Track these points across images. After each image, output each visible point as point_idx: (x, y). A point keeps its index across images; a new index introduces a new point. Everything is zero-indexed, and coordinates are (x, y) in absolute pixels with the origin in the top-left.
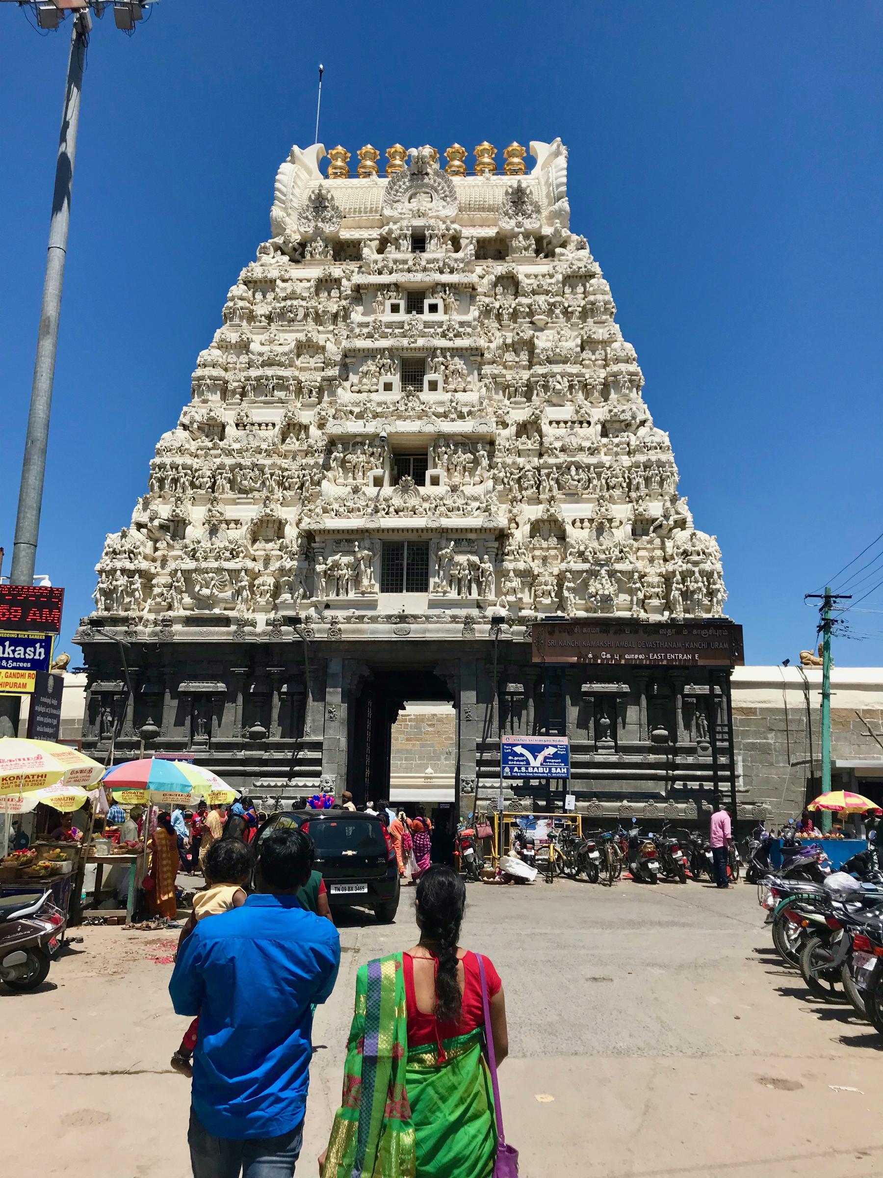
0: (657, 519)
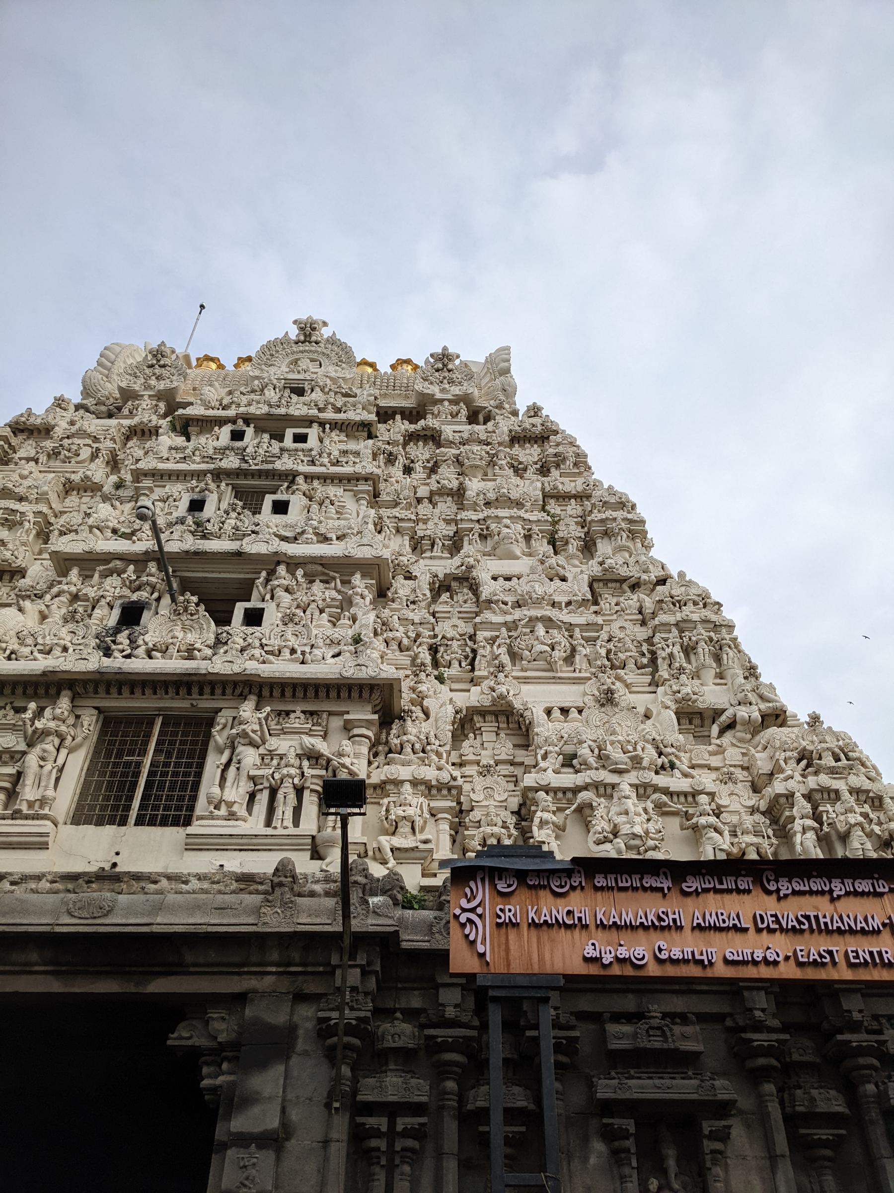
0: (724, 710)
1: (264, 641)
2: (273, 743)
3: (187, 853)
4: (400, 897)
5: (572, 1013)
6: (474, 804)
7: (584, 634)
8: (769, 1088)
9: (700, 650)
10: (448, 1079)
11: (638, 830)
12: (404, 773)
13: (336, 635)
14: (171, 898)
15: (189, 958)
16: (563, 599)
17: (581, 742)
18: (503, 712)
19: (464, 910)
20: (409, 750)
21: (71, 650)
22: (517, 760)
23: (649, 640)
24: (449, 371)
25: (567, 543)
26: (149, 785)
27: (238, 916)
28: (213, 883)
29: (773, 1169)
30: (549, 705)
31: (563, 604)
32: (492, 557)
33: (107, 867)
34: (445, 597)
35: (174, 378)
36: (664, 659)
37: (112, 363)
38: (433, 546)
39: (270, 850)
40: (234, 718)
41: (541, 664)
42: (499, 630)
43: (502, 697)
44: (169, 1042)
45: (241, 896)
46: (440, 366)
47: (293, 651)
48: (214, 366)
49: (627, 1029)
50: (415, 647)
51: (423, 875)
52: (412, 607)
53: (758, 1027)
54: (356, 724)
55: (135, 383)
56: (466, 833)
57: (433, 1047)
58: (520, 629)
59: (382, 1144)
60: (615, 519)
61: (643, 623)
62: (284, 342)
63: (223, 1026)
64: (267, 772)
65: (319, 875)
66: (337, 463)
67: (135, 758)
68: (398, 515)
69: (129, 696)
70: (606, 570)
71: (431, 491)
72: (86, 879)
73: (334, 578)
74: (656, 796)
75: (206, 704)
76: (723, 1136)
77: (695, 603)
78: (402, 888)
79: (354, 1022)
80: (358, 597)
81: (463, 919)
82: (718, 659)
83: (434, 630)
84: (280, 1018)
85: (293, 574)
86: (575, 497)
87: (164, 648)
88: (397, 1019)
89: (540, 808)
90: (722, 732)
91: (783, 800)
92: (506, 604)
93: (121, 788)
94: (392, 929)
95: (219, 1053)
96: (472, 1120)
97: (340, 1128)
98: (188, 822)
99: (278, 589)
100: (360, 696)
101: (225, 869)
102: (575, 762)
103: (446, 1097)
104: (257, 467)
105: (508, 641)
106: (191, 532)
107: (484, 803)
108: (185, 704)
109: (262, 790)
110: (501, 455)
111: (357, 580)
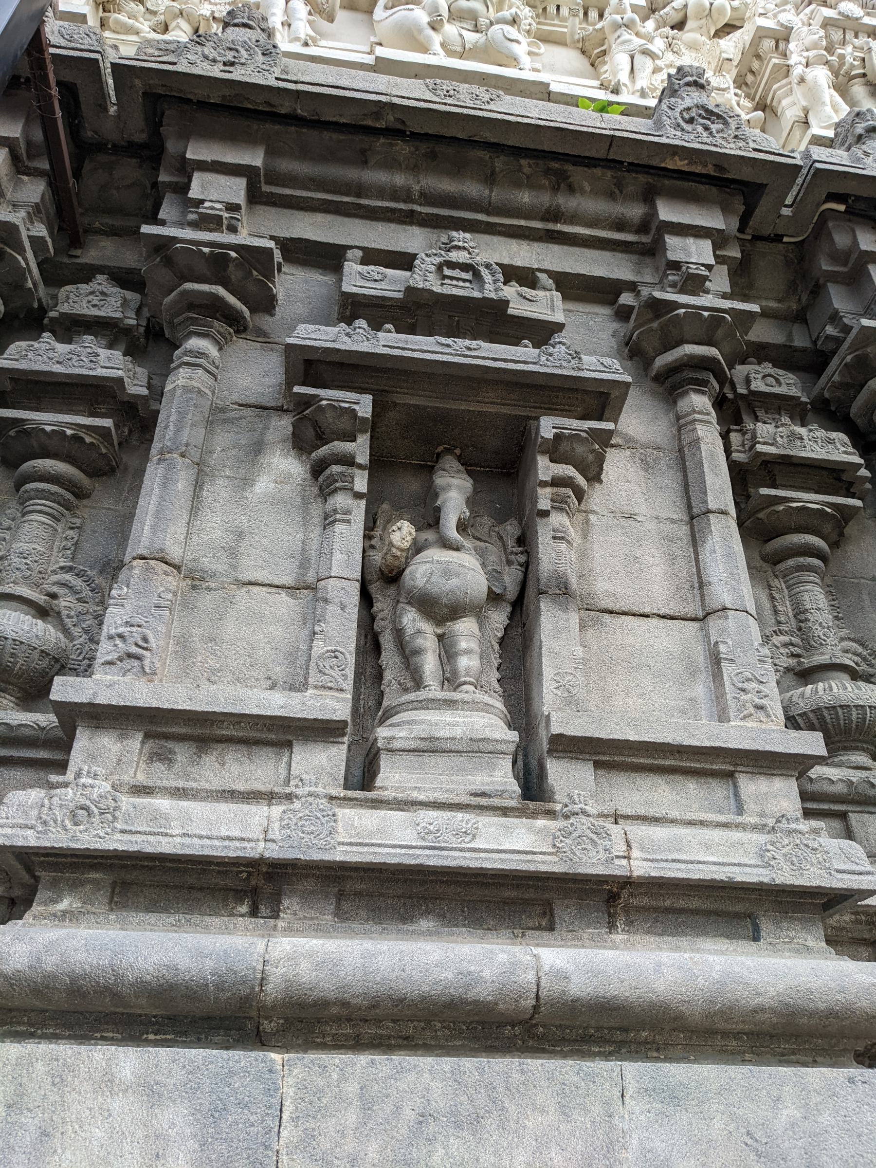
29: (695, 541)
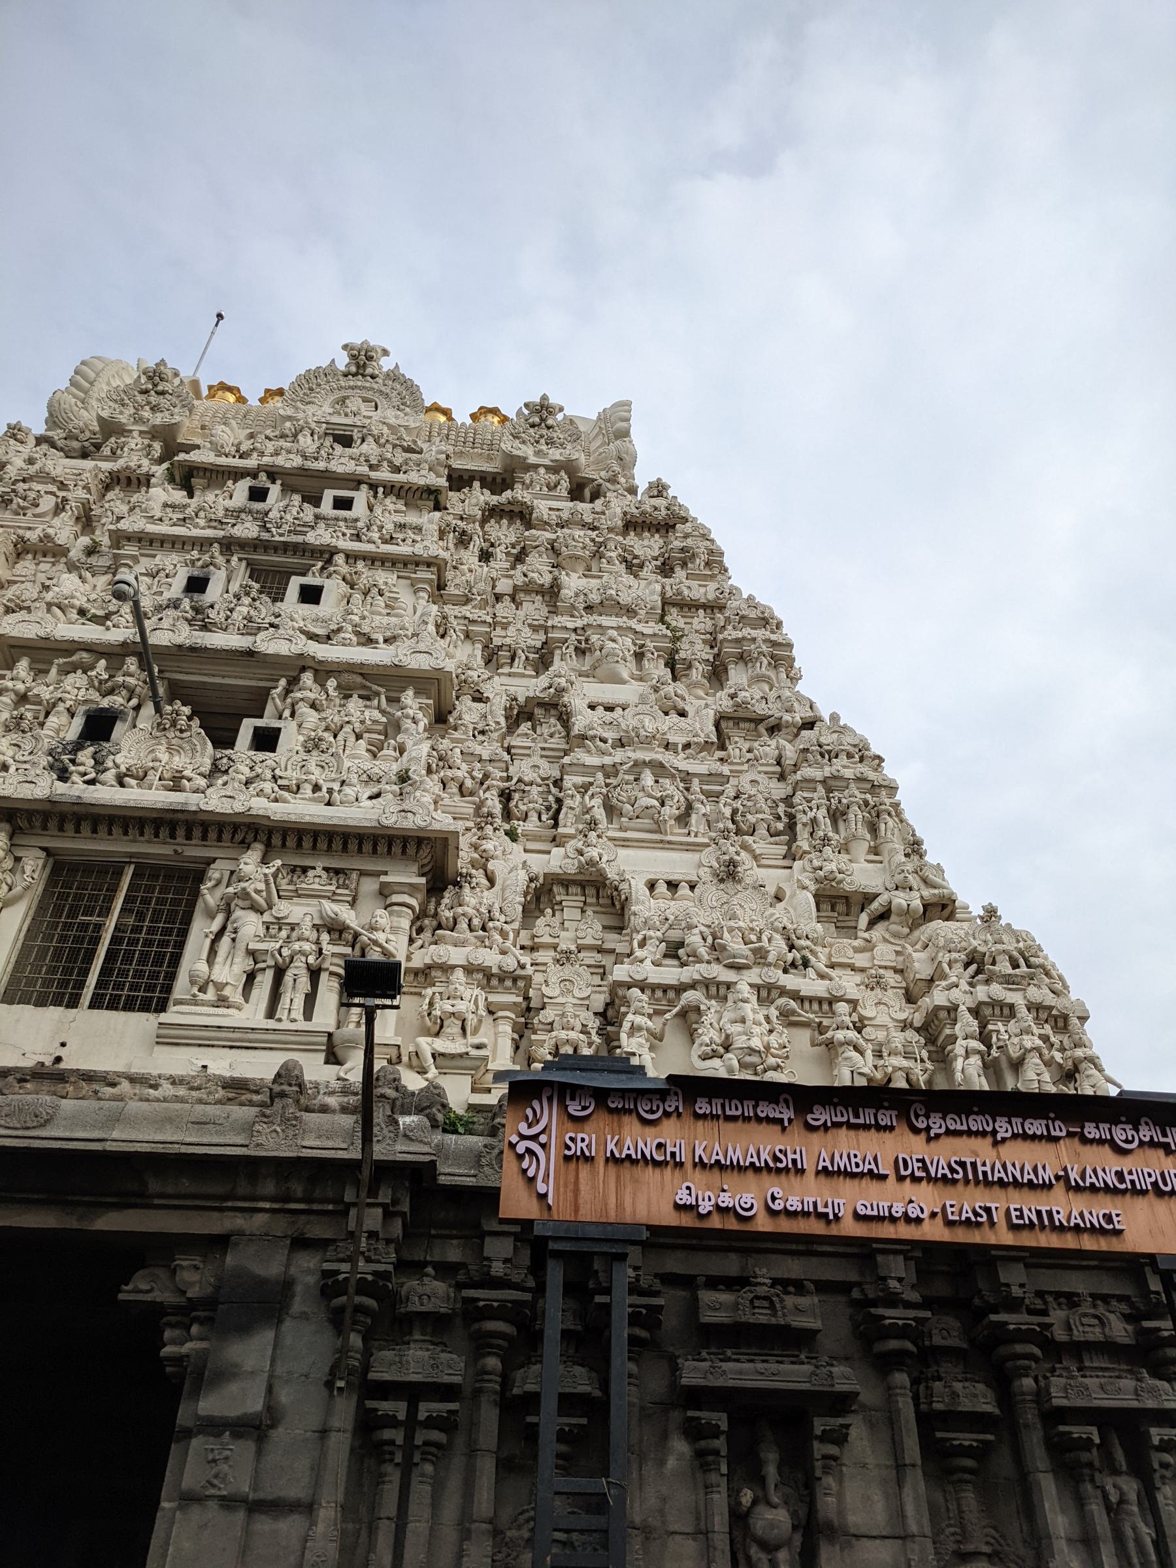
0: (877, 896)
1: (278, 772)
2: (283, 908)
3: (158, 1048)
4: (440, 1117)
5: (656, 1275)
6: (546, 1000)
7: (704, 787)
8: (901, 1378)
9: (851, 816)
10: (489, 1354)
11: (756, 1043)
12: (456, 956)
13: (376, 770)
14: (134, 1106)
15: (154, 1186)
16: (680, 740)
17: (690, 927)
18: (591, 883)
19: (523, 1137)
20: (465, 926)
21: (12, 770)
22: (607, 946)
23: (788, 800)
24: (548, 428)
25: (690, 667)
26: (111, 956)
27: (223, 1133)
28: (192, 1089)
29: (900, 1483)
30: (652, 876)
31: (680, 747)
32: (591, 679)
33: (48, 1061)
34: (525, 727)
35: (176, 410)
36: (805, 825)
37: (91, 383)
38: (513, 659)
39: (271, 1049)
40: (232, 872)
41: (646, 822)
42: (593, 775)
43: (591, 863)
44: (121, 1296)
45: (228, 1108)
46: (537, 420)
47: (316, 788)
48: (231, 398)
49: (725, 1297)
50: (481, 792)
51: (473, 1090)
52: (480, 738)
53: (893, 1300)
54: (396, 888)
55: (121, 413)
56: (534, 1037)
57: (473, 1313)
58: (621, 775)
59: (398, 1436)
60: (754, 640)
61: (782, 777)
62: (329, 372)
63: (195, 1277)
64: (273, 946)
65: (335, 1085)
66: (391, 540)
67: (94, 919)
68: (468, 615)
69: (89, 834)
70: (738, 705)
71: (515, 586)
72: (18, 1076)
73: (378, 694)
74: (782, 1001)
75: (194, 851)
76: (839, 1438)
77: (850, 756)
78: (444, 1106)
79: (370, 1278)
80: (409, 721)
81: (521, 1149)
82: (873, 829)
83: (507, 770)
84: (271, 1267)
85: (323, 685)
86: (704, 607)
87: (141, 774)
88: (427, 1275)
89: (632, 1009)
90: (872, 923)
91: (943, 1014)
92: (604, 741)
93: (73, 957)
94: (427, 1158)
95: (189, 1312)
96: (518, 1409)
97: (344, 1413)
98: (162, 1007)
99: (301, 704)
100: (404, 852)
101: (209, 1071)
102: (681, 952)
103: (487, 1377)
104: (282, 539)
105: (604, 791)
106: (186, 619)
107: (560, 1000)
108: (167, 850)
109: (264, 969)
110: (611, 545)
111: (409, 697)
